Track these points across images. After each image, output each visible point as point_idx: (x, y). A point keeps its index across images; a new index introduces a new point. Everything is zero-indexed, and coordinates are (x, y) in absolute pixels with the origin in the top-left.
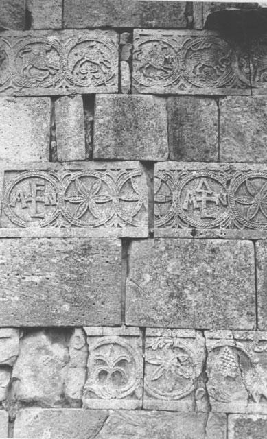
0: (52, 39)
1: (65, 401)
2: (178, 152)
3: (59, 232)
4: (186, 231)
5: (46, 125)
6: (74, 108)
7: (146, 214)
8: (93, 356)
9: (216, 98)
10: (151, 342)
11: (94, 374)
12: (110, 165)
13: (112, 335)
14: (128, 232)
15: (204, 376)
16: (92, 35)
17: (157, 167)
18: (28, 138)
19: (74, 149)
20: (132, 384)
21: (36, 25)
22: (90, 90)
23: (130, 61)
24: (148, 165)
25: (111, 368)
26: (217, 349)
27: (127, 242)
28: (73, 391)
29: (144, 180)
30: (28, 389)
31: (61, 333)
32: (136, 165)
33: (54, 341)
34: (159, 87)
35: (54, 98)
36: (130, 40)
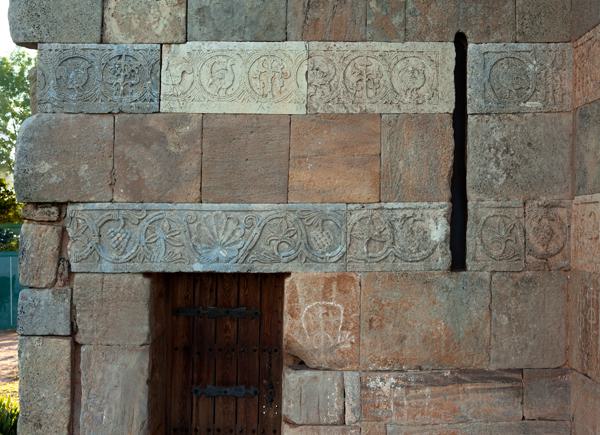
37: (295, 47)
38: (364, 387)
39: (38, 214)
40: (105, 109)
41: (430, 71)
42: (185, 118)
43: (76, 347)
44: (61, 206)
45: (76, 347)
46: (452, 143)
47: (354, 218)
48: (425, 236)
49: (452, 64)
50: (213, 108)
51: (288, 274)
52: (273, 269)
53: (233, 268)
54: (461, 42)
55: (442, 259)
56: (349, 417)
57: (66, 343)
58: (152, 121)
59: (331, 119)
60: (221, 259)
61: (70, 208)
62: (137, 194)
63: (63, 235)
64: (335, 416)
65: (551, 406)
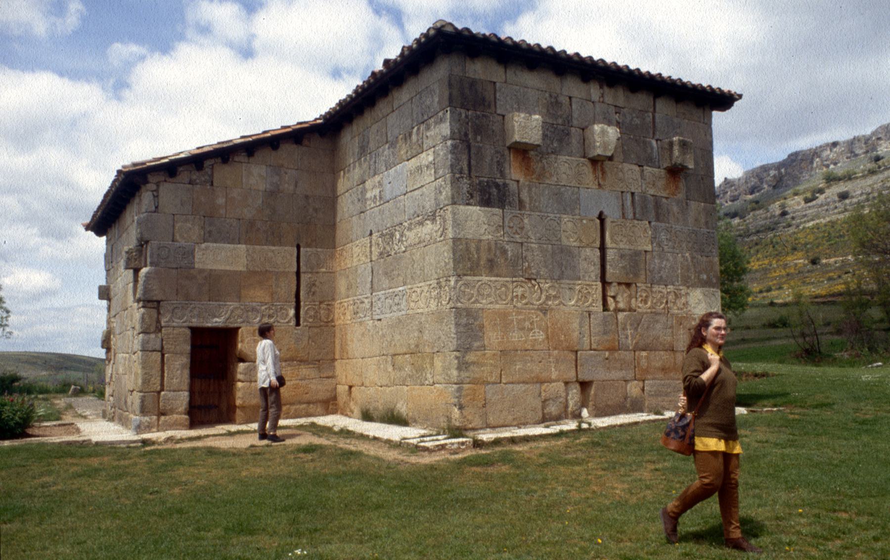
1: (630, 310)
2: (658, 219)
3: (627, 247)
6: (629, 196)
10: (654, 290)
17: (653, 223)
27: (646, 251)
28: (633, 306)
30: (621, 305)
31: (628, 285)
35: (622, 192)
37: (243, 247)
39: (149, 305)
40: (174, 266)
41: (289, 257)
43: (163, 355)
44: (159, 302)
45: (163, 355)
46: (295, 282)
47: (263, 308)
48: (287, 315)
49: (295, 254)
50: (214, 267)
51: (239, 328)
52: (236, 325)
53: (221, 325)
54: (298, 247)
55: (293, 323)
57: (159, 354)
58: (192, 271)
59: (255, 272)
60: (217, 322)
62: (187, 297)
63: (159, 313)
65: (331, 374)
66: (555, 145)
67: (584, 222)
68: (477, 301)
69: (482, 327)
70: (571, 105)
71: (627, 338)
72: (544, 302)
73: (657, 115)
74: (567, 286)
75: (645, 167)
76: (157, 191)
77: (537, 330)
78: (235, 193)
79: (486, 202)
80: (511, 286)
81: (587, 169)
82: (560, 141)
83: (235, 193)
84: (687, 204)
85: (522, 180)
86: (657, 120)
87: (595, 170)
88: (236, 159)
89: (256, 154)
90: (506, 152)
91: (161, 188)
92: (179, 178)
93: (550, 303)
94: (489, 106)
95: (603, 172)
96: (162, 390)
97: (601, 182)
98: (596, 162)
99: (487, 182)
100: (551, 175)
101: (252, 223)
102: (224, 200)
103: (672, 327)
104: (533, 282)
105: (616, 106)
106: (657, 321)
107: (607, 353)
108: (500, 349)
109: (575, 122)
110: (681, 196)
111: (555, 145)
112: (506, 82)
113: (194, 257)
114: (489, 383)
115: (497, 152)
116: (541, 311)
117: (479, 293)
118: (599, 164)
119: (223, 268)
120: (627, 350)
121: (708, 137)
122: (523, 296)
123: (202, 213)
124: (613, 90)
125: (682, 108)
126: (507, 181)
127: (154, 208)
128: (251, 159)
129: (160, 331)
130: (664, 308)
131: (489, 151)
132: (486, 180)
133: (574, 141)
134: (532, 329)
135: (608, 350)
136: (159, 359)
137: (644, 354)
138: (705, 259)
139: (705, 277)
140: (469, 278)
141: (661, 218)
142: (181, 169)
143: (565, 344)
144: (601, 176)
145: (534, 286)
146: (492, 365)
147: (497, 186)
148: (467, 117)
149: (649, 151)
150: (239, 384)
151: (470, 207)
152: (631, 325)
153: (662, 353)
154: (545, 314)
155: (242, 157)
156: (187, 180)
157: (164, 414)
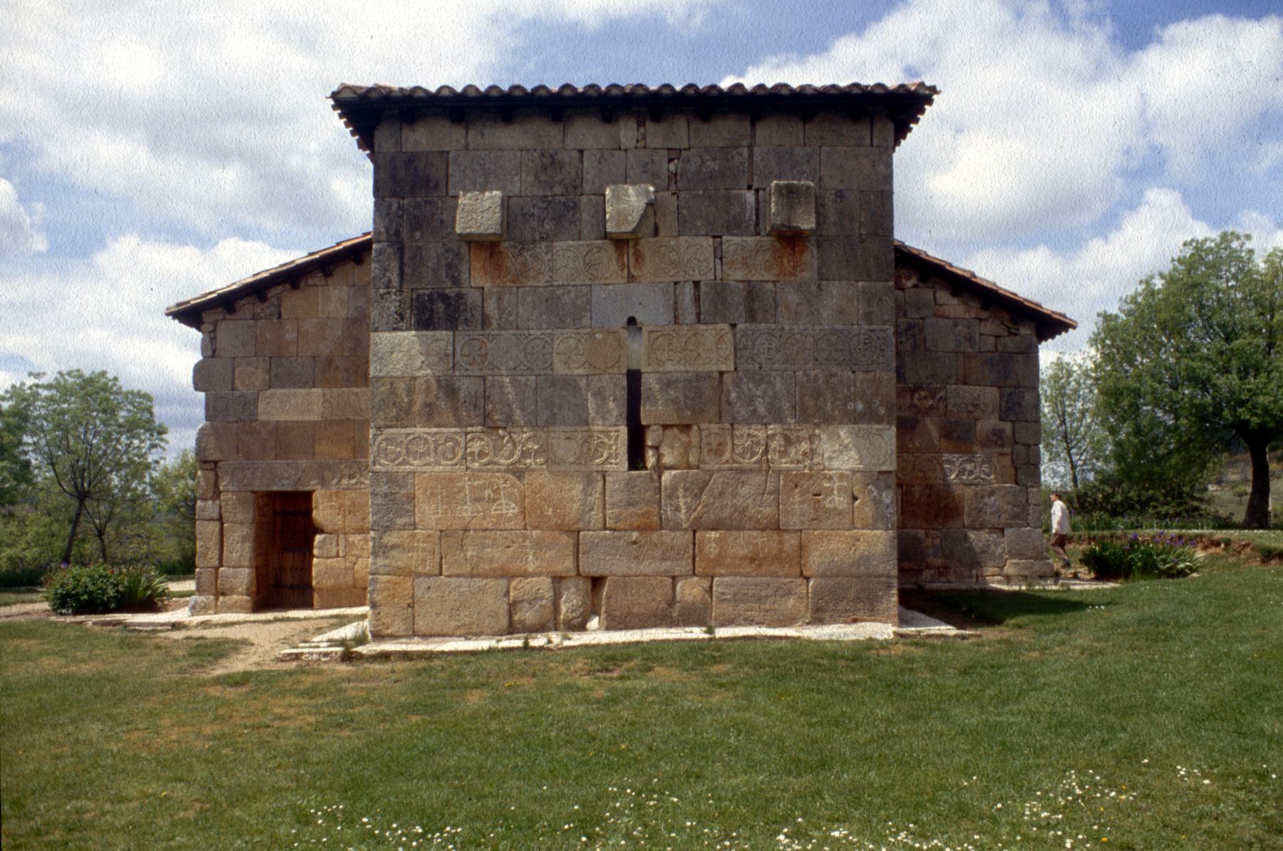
0: (673, 243)
2: (752, 317)
3: (682, 368)
4: (757, 366)
5: (671, 302)
6: (689, 289)
7: (732, 357)
8: (705, 441)
9: (774, 282)
10: (737, 433)
11: (705, 453)
12: (710, 327)
13: (714, 427)
14: (724, 368)
15: (766, 452)
16: (697, 240)
17: (740, 326)
18: (662, 310)
19: (689, 315)
20: (727, 455)
21: (662, 232)
22: (697, 278)
23: (721, 259)
24: (733, 326)
25: (714, 447)
26: (774, 435)
27: (721, 373)
29: (730, 336)
31: (686, 428)
32: (726, 327)
33: (682, 432)
34: (739, 275)
35: (676, 283)
36: (721, 244)
38: (347, 540)
39: (205, 466)
42: (269, 422)
43: (222, 524)
44: (216, 463)
50: (282, 419)
53: (289, 489)
56: (341, 554)
58: (254, 424)
60: (285, 486)
61: (220, 464)
62: (248, 456)
63: (217, 476)
64: (334, 553)
66: (547, 227)
67: (599, 336)
68: (404, 463)
69: (411, 498)
70: (581, 161)
71: (677, 509)
72: (519, 461)
73: (757, 150)
74: (562, 436)
75: (725, 238)
76: (214, 331)
77: (503, 501)
78: (309, 325)
79: (425, 322)
80: (462, 440)
81: (608, 254)
82: (558, 220)
83: (309, 325)
84: (819, 287)
85: (487, 286)
86: (757, 158)
87: (620, 257)
88: (311, 282)
89: (335, 273)
90: (464, 249)
91: (219, 329)
92: (239, 315)
93: (529, 461)
94: (436, 187)
95: (639, 257)
96: (221, 565)
97: (634, 272)
98: (620, 243)
99: (430, 296)
100: (539, 273)
101: (329, 361)
102: (295, 335)
103: (776, 491)
104: (501, 432)
105: (669, 150)
106: (743, 483)
107: (635, 535)
108: (439, 527)
109: (587, 187)
110: (807, 274)
111: (547, 227)
112: (467, 149)
113: (256, 407)
114: (419, 575)
115: (448, 251)
116: (514, 473)
117: (408, 453)
118: (631, 244)
119: (295, 418)
120: (677, 527)
121: (881, 168)
122: (482, 454)
123: (268, 353)
124: (663, 126)
125: (813, 129)
126: (464, 291)
127: (210, 353)
128: (330, 281)
129: (218, 496)
130: (759, 461)
131: (433, 251)
132: (427, 292)
133: (585, 216)
134: (495, 500)
135: (638, 529)
136: (217, 529)
137: (713, 535)
138: (860, 376)
139: (860, 406)
140: (391, 430)
141: (760, 315)
142: (242, 302)
143: (554, 520)
144: (632, 262)
145: (503, 437)
146: (424, 550)
147: (445, 298)
148: (400, 208)
149: (735, 209)
150: (315, 560)
151: (399, 333)
152: (686, 490)
153: (755, 533)
154: (519, 478)
155: (317, 279)
156: (249, 315)
157: (224, 594)
